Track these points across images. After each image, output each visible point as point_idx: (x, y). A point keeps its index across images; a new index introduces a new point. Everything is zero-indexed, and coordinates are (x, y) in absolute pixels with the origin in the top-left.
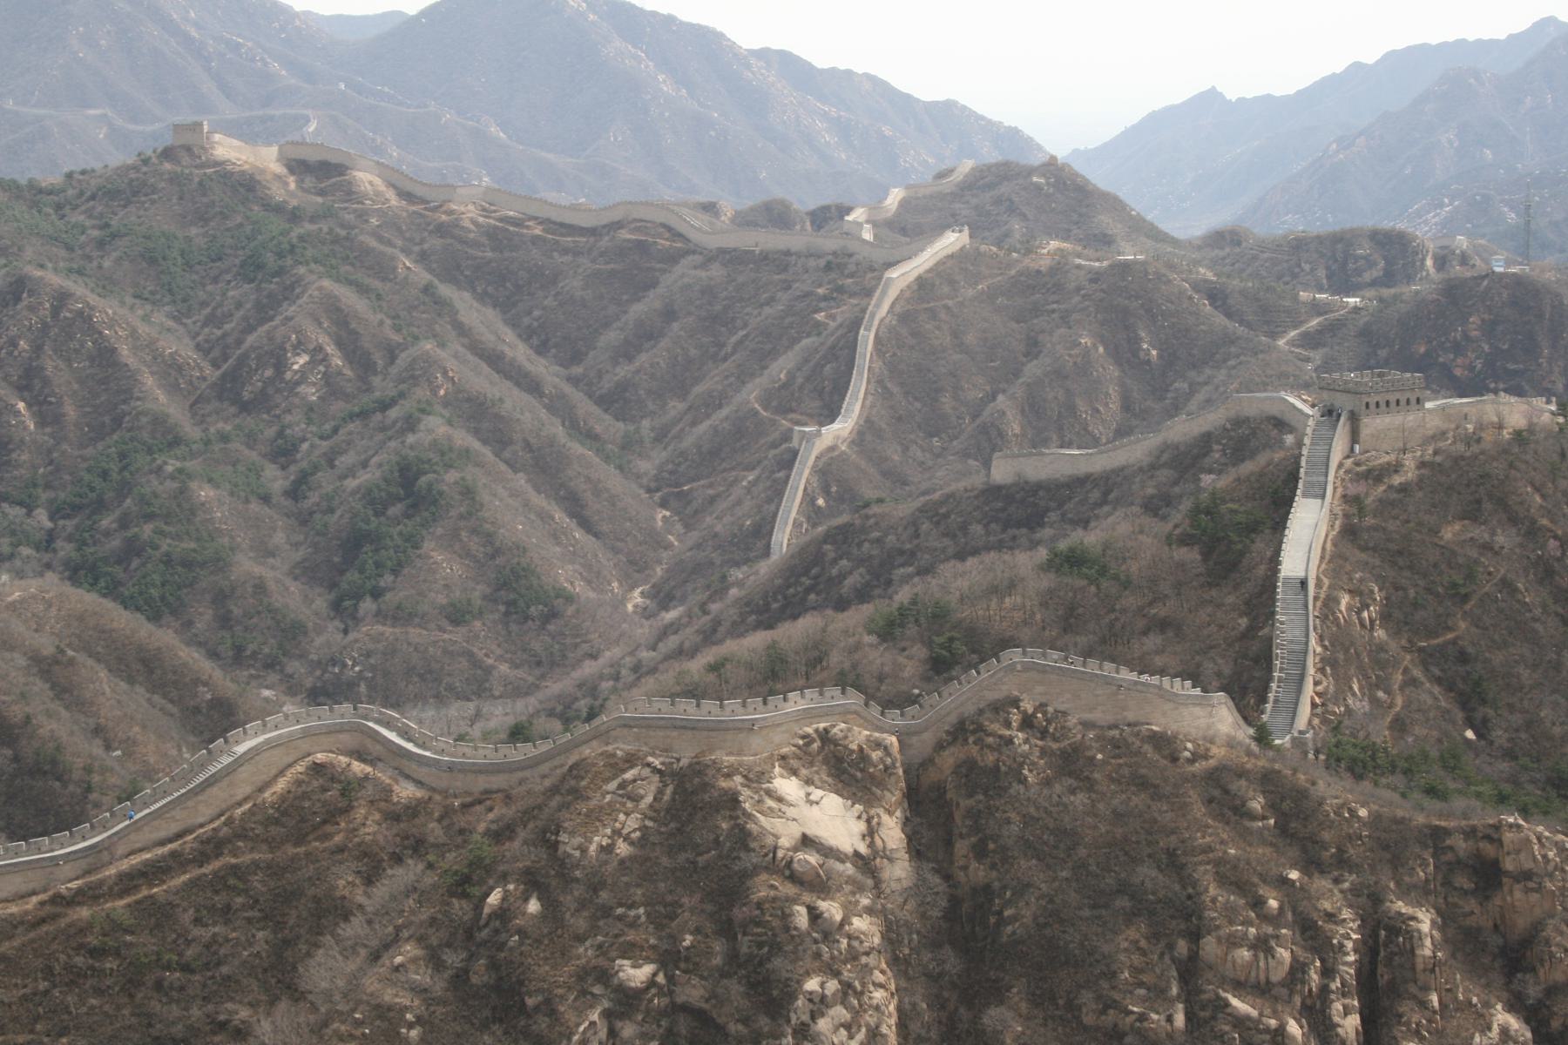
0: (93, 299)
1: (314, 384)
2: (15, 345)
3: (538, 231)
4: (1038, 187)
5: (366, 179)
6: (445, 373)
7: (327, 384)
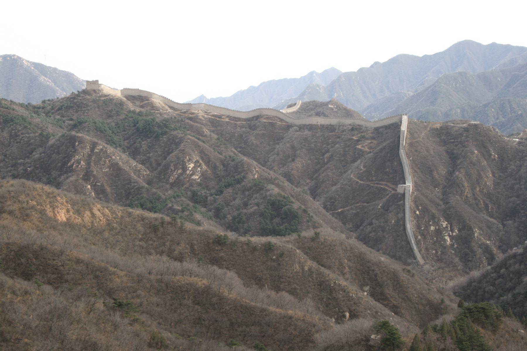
1: (198, 175)
3: (227, 120)
4: (332, 109)
6: (255, 169)
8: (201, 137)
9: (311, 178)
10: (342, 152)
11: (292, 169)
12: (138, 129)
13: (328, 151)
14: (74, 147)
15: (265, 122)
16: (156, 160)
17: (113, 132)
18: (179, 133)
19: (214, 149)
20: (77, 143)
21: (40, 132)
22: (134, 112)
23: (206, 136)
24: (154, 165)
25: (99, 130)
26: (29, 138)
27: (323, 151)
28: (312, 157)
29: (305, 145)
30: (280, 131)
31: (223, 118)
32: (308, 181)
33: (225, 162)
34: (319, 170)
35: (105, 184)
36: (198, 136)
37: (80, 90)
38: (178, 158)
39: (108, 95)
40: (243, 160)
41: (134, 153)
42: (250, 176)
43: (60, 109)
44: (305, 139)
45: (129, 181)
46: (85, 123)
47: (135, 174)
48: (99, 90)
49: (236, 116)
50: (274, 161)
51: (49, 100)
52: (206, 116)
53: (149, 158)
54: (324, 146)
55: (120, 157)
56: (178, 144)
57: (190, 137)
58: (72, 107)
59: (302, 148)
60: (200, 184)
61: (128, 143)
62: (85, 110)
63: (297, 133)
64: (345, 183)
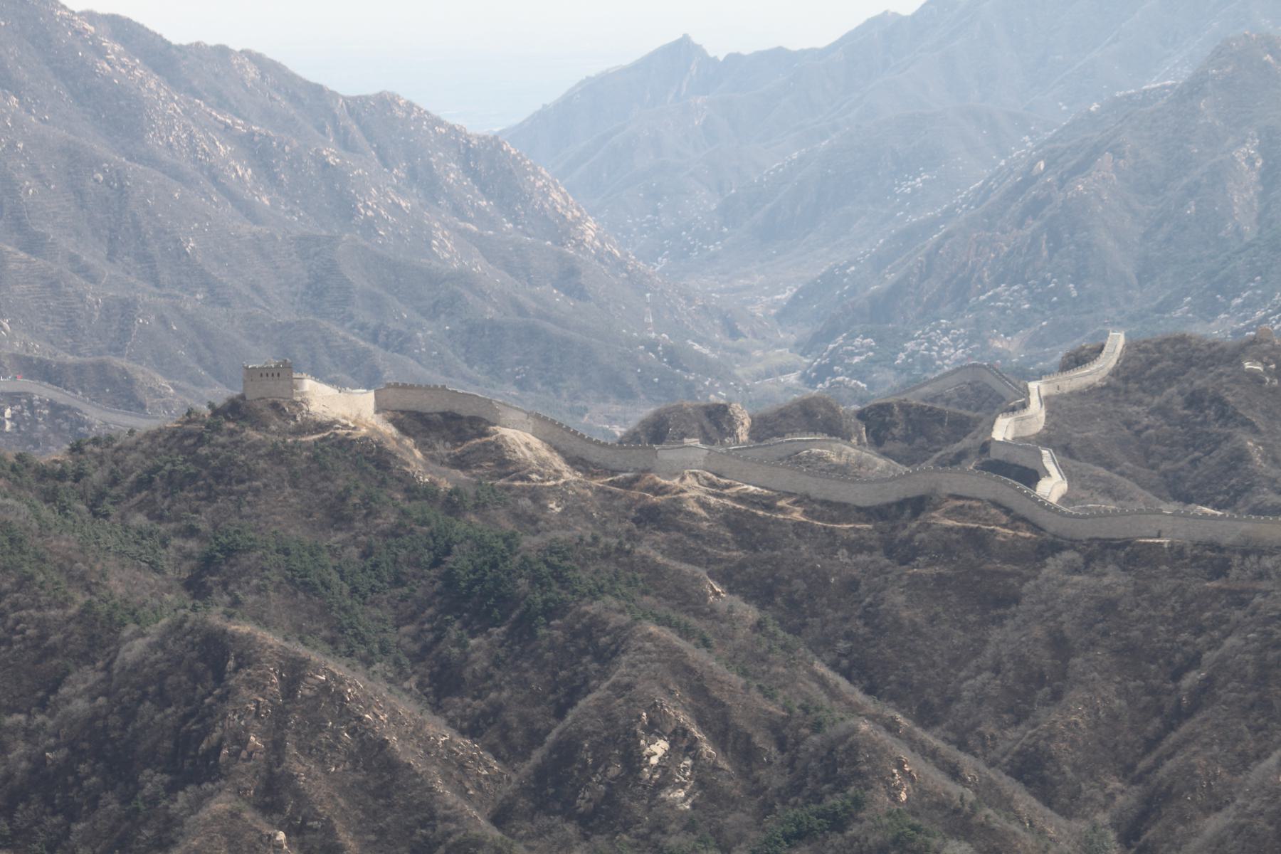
0: (338, 667)
1: (682, 786)
2: (244, 743)
3: (797, 515)
4: (1255, 378)
5: (520, 438)
6: (900, 766)
7: (701, 784)
8: (693, 621)
9: (1127, 772)
10: (1250, 669)
11: (1051, 737)
12: (449, 579)
13: (1194, 661)
14: (220, 678)
15: (949, 530)
16: (523, 719)
17: (354, 590)
18: (607, 609)
19: (744, 673)
20: (231, 664)
21: (80, 598)
22: (429, 493)
23: (712, 614)
24: (518, 736)
25: (302, 584)
26: (41, 624)
27: (1178, 658)
28: (1131, 684)
29: (1105, 634)
30: (1008, 568)
31: (782, 510)
32: (1115, 784)
33: (786, 731)
34: (1159, 738)
35: (339, 825)
36: (684, 618)
37: (219, 403)
38: (610, 719)
39: (330, 425)
40: (854, 730)
41: (442, 685)
42: (881, 799)
43: (144, 483)
44: (1108, 607)
45: (427, 813)
46: (249, 549)
47: (447, 777)
48: (295, 403)
49: (835, 498)
50: (979, 700)
51: (96, 441)
52: (713, 500)
53: (497, 709)
54: (1184, 636)
55: (391, 708)
56: (606, 657)
57: (653, 629)
58: (193, 478)
59: (1093, 643)
60: (690, 826)
61: (415, 638)
62: (243, 493)
63: (1076, 578)
64: (1254, 806)
